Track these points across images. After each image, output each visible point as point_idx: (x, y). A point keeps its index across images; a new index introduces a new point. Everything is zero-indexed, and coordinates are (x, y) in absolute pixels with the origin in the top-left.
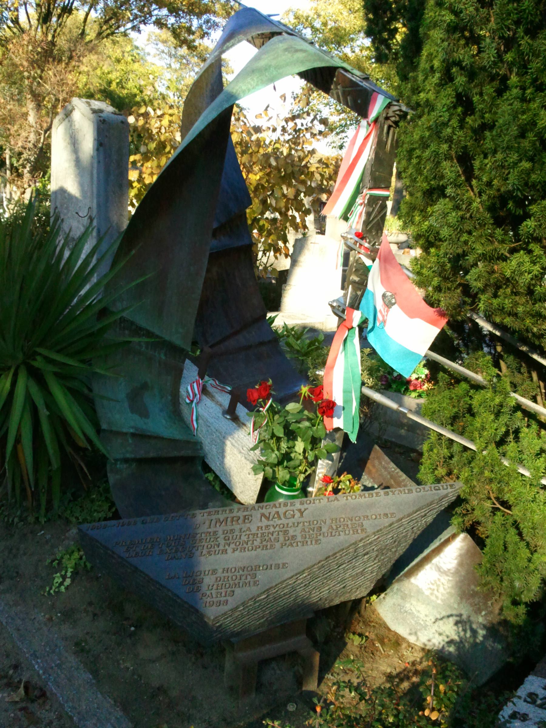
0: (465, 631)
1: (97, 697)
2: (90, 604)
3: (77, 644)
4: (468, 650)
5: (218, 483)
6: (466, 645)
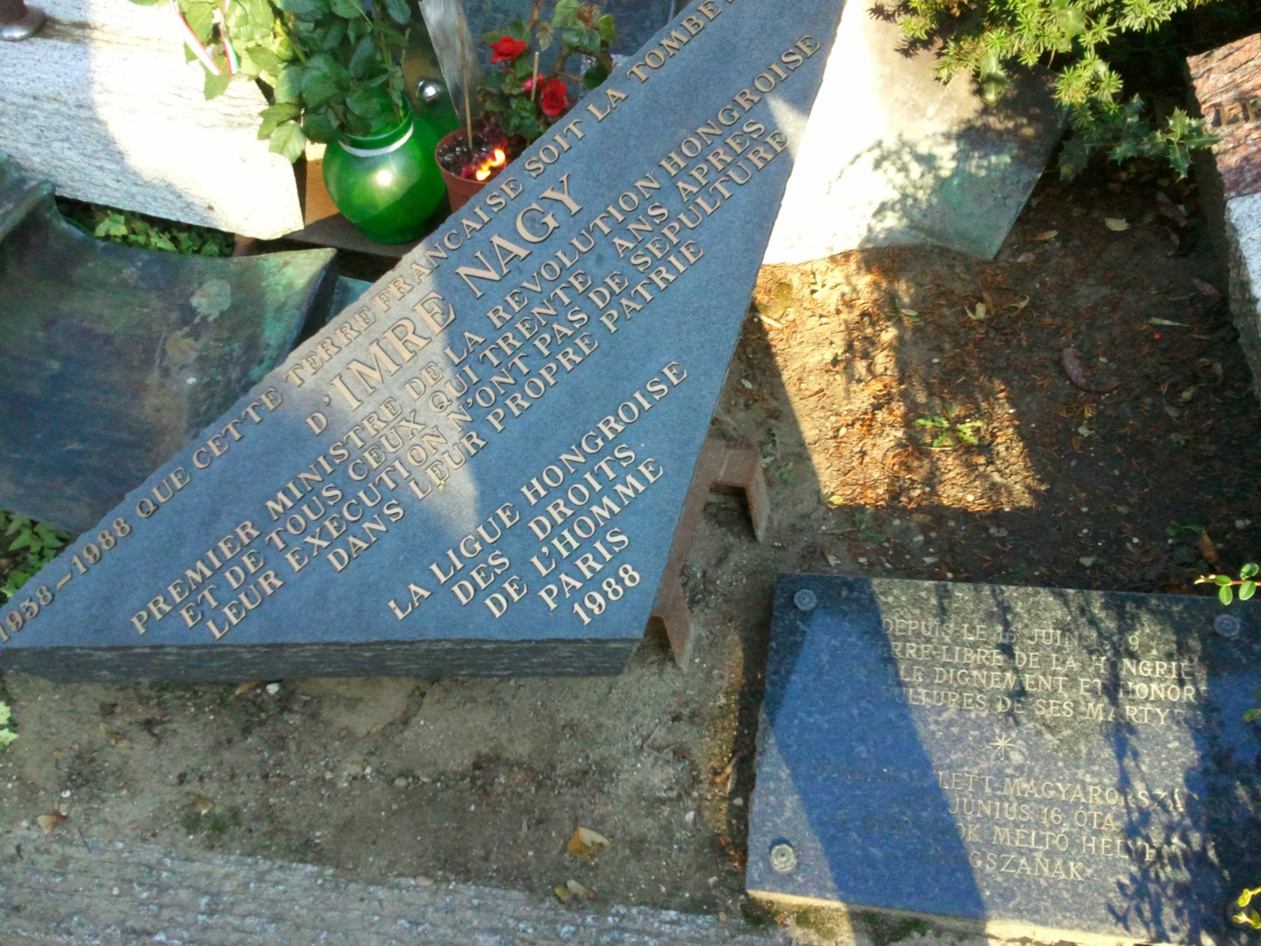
0: (904, 169)
1: (380, 901)
2: (108, 710)
3: (192, 823)
4: (930, 206)
5: (139, 225)
6: (920, 194)
